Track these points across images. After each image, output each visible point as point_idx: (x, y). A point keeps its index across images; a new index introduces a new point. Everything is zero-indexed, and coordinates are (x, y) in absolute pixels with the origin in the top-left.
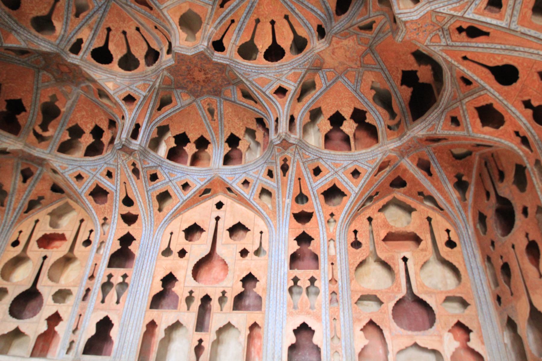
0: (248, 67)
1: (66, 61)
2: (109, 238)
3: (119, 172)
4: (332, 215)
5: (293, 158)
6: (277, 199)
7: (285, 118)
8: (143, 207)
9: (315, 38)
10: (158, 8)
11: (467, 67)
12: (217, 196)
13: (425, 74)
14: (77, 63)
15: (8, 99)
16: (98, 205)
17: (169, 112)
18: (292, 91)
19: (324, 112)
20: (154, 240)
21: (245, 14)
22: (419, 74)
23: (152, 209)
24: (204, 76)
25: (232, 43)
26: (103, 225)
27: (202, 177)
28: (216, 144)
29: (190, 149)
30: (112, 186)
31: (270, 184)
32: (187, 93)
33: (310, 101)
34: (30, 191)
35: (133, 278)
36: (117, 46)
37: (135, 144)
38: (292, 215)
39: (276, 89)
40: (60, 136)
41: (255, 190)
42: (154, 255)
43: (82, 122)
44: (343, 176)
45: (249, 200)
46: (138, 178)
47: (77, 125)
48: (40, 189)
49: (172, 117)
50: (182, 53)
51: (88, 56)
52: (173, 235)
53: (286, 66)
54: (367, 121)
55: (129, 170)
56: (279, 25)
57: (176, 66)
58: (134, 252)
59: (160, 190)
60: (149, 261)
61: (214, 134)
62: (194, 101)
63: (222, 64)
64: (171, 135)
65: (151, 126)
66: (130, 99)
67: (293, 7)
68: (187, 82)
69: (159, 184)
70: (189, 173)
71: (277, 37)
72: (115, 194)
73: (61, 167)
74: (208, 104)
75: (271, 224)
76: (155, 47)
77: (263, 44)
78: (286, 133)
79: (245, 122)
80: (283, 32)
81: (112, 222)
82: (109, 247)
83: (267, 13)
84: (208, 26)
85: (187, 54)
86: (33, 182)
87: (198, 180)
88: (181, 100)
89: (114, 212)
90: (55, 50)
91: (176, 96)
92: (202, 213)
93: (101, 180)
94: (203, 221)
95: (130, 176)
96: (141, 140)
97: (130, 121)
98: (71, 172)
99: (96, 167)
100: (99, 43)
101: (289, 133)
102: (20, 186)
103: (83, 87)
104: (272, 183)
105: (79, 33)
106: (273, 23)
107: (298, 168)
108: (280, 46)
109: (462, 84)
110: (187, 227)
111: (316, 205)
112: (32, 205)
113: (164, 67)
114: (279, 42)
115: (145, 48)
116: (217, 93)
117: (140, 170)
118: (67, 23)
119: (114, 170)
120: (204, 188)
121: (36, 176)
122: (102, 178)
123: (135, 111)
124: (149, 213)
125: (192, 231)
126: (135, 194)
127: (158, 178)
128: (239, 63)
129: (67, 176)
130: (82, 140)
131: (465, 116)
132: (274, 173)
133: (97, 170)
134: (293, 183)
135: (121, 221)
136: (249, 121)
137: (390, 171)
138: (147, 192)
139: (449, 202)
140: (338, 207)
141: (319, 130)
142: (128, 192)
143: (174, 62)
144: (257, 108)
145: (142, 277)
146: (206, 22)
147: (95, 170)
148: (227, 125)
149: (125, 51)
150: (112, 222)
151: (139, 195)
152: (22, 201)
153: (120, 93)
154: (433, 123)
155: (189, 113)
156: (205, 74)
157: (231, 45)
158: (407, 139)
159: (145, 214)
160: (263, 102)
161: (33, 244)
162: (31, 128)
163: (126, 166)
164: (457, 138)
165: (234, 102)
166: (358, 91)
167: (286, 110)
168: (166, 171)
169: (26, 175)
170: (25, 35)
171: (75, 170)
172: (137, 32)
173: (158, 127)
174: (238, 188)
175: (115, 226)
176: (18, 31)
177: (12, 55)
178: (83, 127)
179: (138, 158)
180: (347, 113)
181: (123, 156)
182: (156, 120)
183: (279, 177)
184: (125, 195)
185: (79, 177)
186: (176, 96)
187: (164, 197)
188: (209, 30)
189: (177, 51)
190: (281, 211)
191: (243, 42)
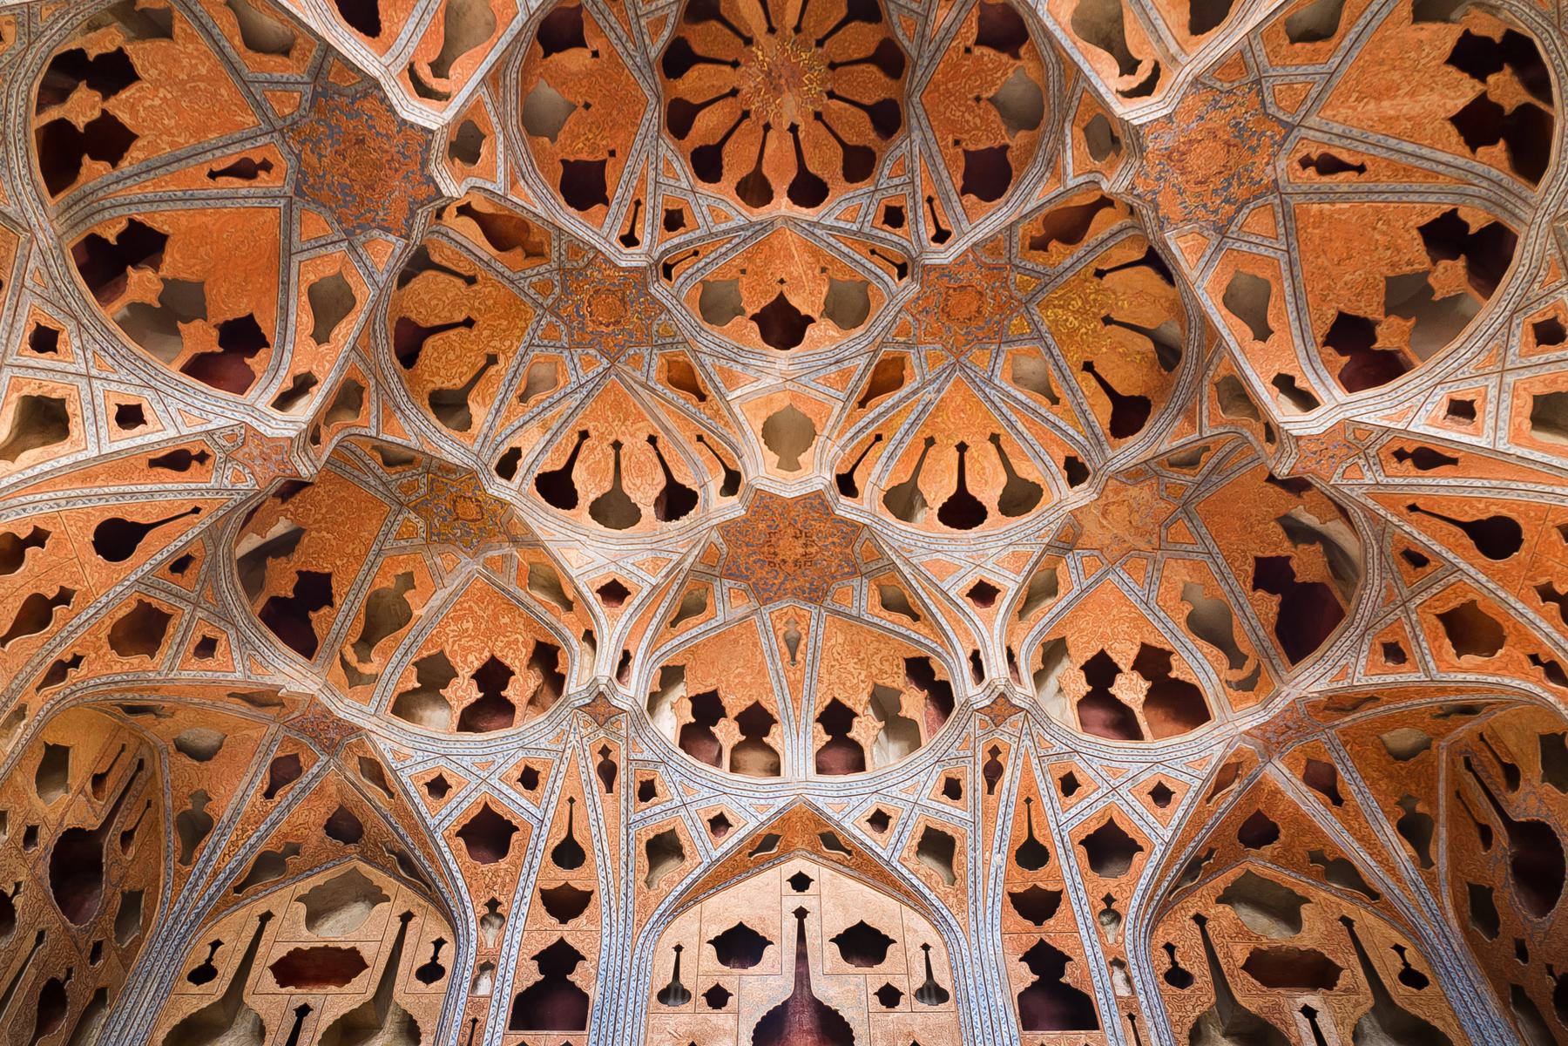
3: (563, 768)
4: (1109, 899)
6: (970, 854)
9: (1063, 483)
10: (722, 397)
11: (1419, 525)
13: (1308, 565)
17: (694, 632)
18: (1011, 593)
19: (1072, 651)
22: (1294, 564)
23: (631, 877)
25: (875, 480)
29: (727, 733)
30: (532, 809)
31: (952, 817)
33: (1046, 620)
34: (273, 824)
36: (592, 473)
38: (1008, 899)
40: (395, 678)
41: (907, 834)
44: (1130, 798)
45: (888, 863)
46: (610, 789)
47: (442, 652)
49: (697, 646)
51: (530, 485)
54: (1173, 675)
59: (659, 827)
61: (788, 697)
66: (614, 592)
67: (1013, 418)
69: (657, 809)
71: (968, 479)
72: (536, 831)
73: (394, 752)
75: (953, 923)
79: (874, 671)
87: (752, 810)
89: (522, 884)
92: (758, 900)
94: (762, 919)
97: (614, 641)
98: (420, 768)
99: (490, 758)
104: (958, 812)
105: (517, 435)
106: (962, 448)
107: (1027, 770)
108: (974, 498)
109: (1406, 565)
111: (1068, 870)
112: (269, 866)
113: (715, 522)
114: (972, 488)
115: (660, 481)
116: (815, 595)
118: (498, 411)
119: (548, 764)
120: (764, 831)
121: (305, 779)
122: (504, 788)
123: (624, 619)
125: (740, 946)
126: (594, 830)
131: (1416, 637)
133: (493, 768)
134: (1011, 810)
135: (543, 910)
136: (886, 667)
137: (1240, 793)
138: (628, 827)
139: (1392, 870)
140: (1123, 879)
141: (1060, 690)
146: (826, 433)
147: (483, 767)
149: (607, 486)
154: (1343, 662)
155: (736, 641)
156: (806, 545)
157: (869, 486)
158: (1281, 706)
160: (939, 616)
161: (262, 978)
162: (337, 647)
164: (1401, 692)
165: (858, 618)
166: (1152, 604)
167: (997, 632)
168: (676, 777)
169: (284, 772)
171: (430, 765)
173: (662, 668)
174: (857, 833)
175: (520, 924)
177: (376, 463)
178: (456, 662)
179: (623, 732)
180: (1124, 654)
182: (663, 649)
183: (979, 794)
184: (564, 835)
185: (438, 787)
187: (663, 848)
190: (980, 887)
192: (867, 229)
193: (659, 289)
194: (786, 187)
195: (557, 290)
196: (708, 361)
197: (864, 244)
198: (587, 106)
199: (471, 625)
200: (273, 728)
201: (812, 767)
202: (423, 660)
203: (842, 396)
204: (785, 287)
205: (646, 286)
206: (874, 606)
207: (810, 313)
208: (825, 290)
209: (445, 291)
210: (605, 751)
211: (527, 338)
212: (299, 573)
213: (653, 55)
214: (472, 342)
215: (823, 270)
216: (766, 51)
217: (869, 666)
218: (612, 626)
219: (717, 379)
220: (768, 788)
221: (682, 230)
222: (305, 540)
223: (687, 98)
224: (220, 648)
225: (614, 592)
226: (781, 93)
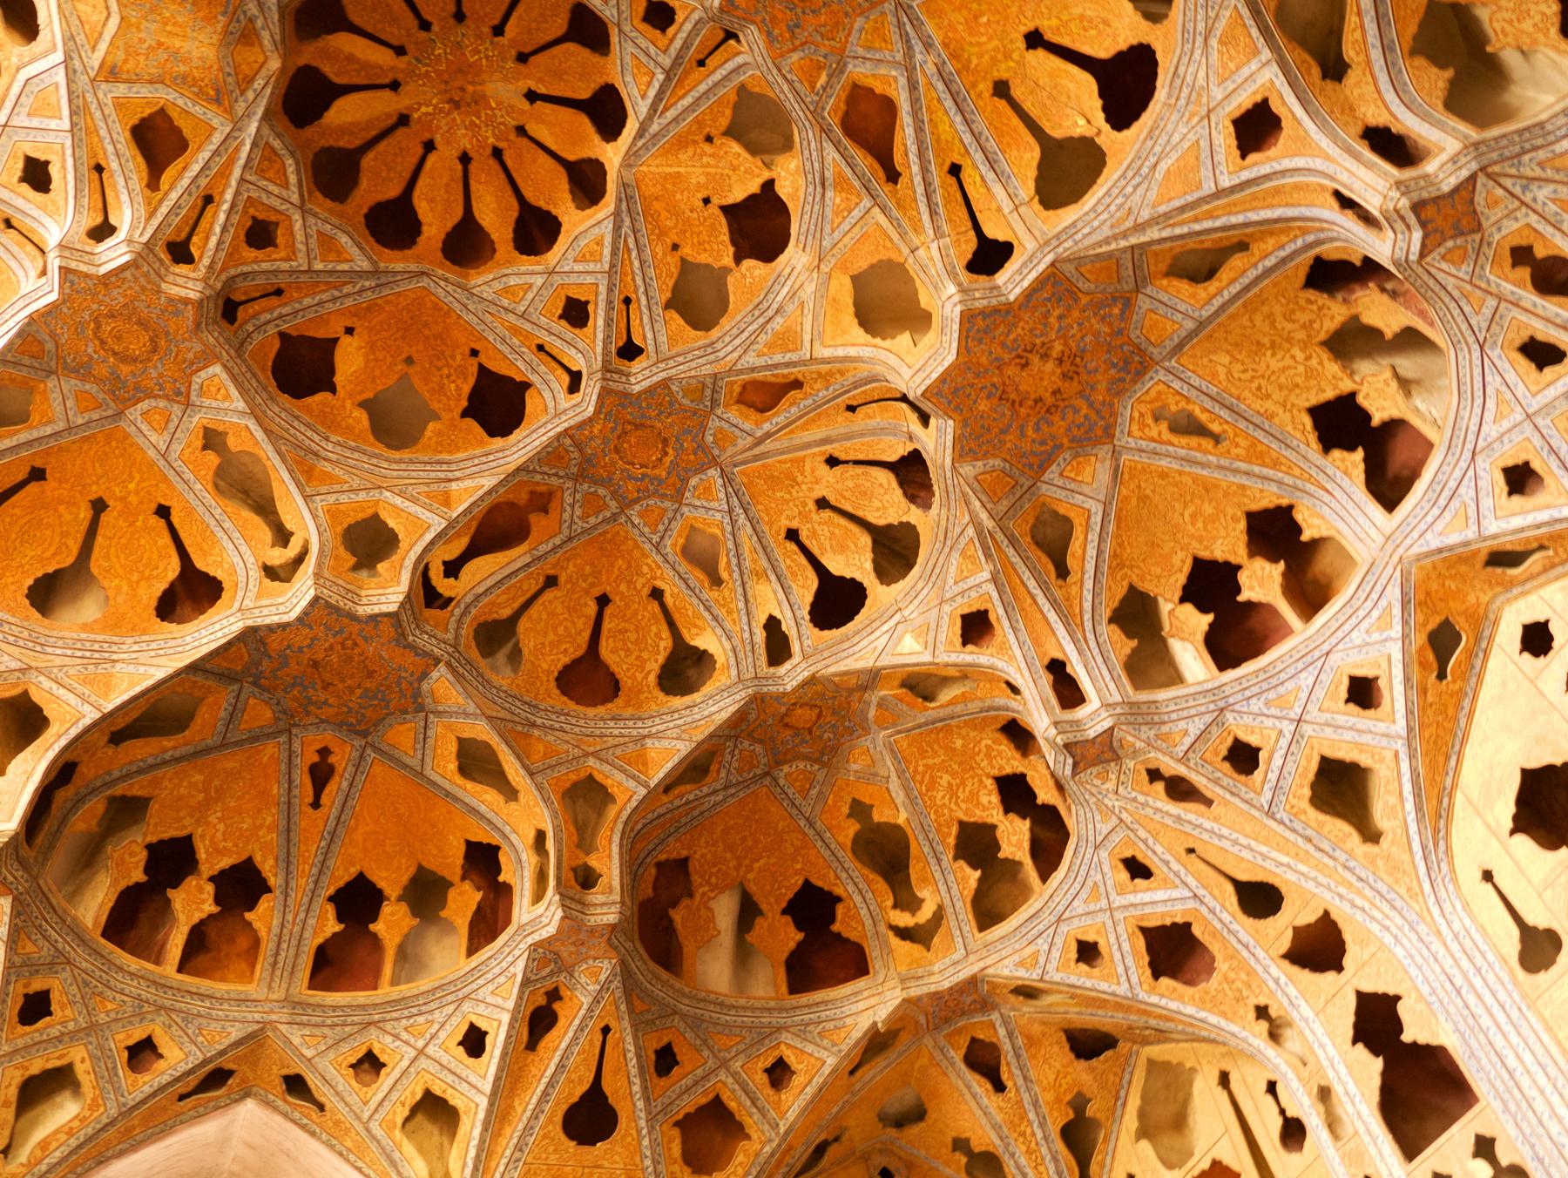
0: (1108, 200)
1: (784, 694)
2: (1325, 1063)
3: (1142, 833)
5: (1533, 218)
7: (1350, 163)
8: (1313, 874)
12: (1496, 622)
14: (806, 674)
15: (784, 904)
16: (1203, 985)
17: (1091, 552)
18: (1281, 82)
20: (1454, 946)
21: (958, 119)
23: (1342, 856)
24: (1050, 366)
26: (1274, 1036)
27: (1375, 613)
28: (1309, 487)
29: (1261, 582)
30: (1175, 894)
32: (1077, 455)
34: (1035, 1104)
35: (1512, 1131)
36: (842, 549)
37: (1093, 717)
39: (1234, 143)
40: (955, 891)
42: (1502, 996)
43: (964, 806)
46: (1208, 803)
47: (962, 825)
48: (1052, 1077)
49: (1115, 556)
50: (935, 376)
52: (1496, 879)
53: (1185, 60)
55: (1159, 804)
56: (1054, 22)
57: (965, 423)
58: (1434, 1042)
60: (1508, 1028)
61: (1266, 471)
62: (1115, 454)
63: (1041, 282)
64: (1170, 606)
65: (1090, 636)
66: (975, 627)
68: (1037, 429)
69: (1277, 762)
70: (1326, 647)
72: (1204, 910)
73: (1021, 964)
74: (1156, 419)
76: (896, 450)
77: (1077, 107)
78: (1398, 184)
80: (1082, 17)
81: (1285, 1002)
82: (1352, 1089)
83: (996, 42)
84: (921, 252)
85: (946, 364)
86: (1017, 1072)
87: (1376, 636)
88: (1085, 489)
89: (1259, 969)
90: (743, 694)
91: (1061, 494)
93: (1134, 905)
95: (1178, 819)
96: (1098, 691)
97: (1027, 674)
98: (1056, 954)
99: (1089, 883)
100: (806, 588)
101: (1408, 173)
102: (1001, 1109)
103: (877, 717)
105: (754, 611)
106: (1035, 40)
110: (1512, 809)
113: (948, 462)
114: (1102, 49)
115: (885, 478)
117: (1182, 770)
119: (1128, 842)
120: (1419, 639)
121: (1006, 1046)
122: (1132, 898)
124: (1348, 875)
126: (1246, 854)
127: (1258, 750)
128: (1074, 224)
129: (1057, 977)
130: (1006, 852)
132: (1547, 333)
133: (1102, 888)
135: (1306, 975)
136: (1303, 317)
138: (1270, 814)
142: (1224, 868)
143: (951, 422)
144: (1267, 254)
145: (1539, 1105)
146: (906, 251)
148: (1269, 405)
149: (866, 540)
150: (1285, 1002)
151: (1264, 849)
152: (1044, 1150)
153: (942, 637)
155: (1143, 499)
156: (1045, 357)
159: (1342, 890)
160: (1253, 216)
162: (882, 928)
163: (1141, 798)
165: (1201, 325)
167: (1325, 143)
168: (1256, 705)
170: (671, 725)
172: (839, 469)
173: (1111, 621)
174: (1516, 522)
175: (1306, 1011)
176: (654, 730)
177: (690, 792)
178: (978, 816)
181: (1106, 780)
182: (1087, 606)
186: (1061, 494)
188: (932, 259)
189: (923, 388)
191: (1032, 173)
192: (667, 61)
193: (641, 376)
194: (596, 139)
195: (601, 491)
196: (751, 359)
197: (686, 73)
198: (409, 360)
199: (946, 778)
200: (928, 1041)
201: (1375, 510)
202: (957, 847)
203: (867, 202)
204: (716, 201)
205: (626, 395)
206: (1193, 296)
207: (760, 181)
208: (736, 147)
209: (552, 614)
210: (1154, 775)
211: (647, 547)
212: (784, 912)
213: (366, 265)
214: (627, 606)
215: (709, 139)
216: (421, 99)
217: (1289, 340)
218: (1011, 658)
219: (778, 358)
220: (1362, 595)
221: (591, 308)
222: (752, 888)
223: (450, 225)
224: (791, 1059)
225: (975, 627)
226: (484, 97)
